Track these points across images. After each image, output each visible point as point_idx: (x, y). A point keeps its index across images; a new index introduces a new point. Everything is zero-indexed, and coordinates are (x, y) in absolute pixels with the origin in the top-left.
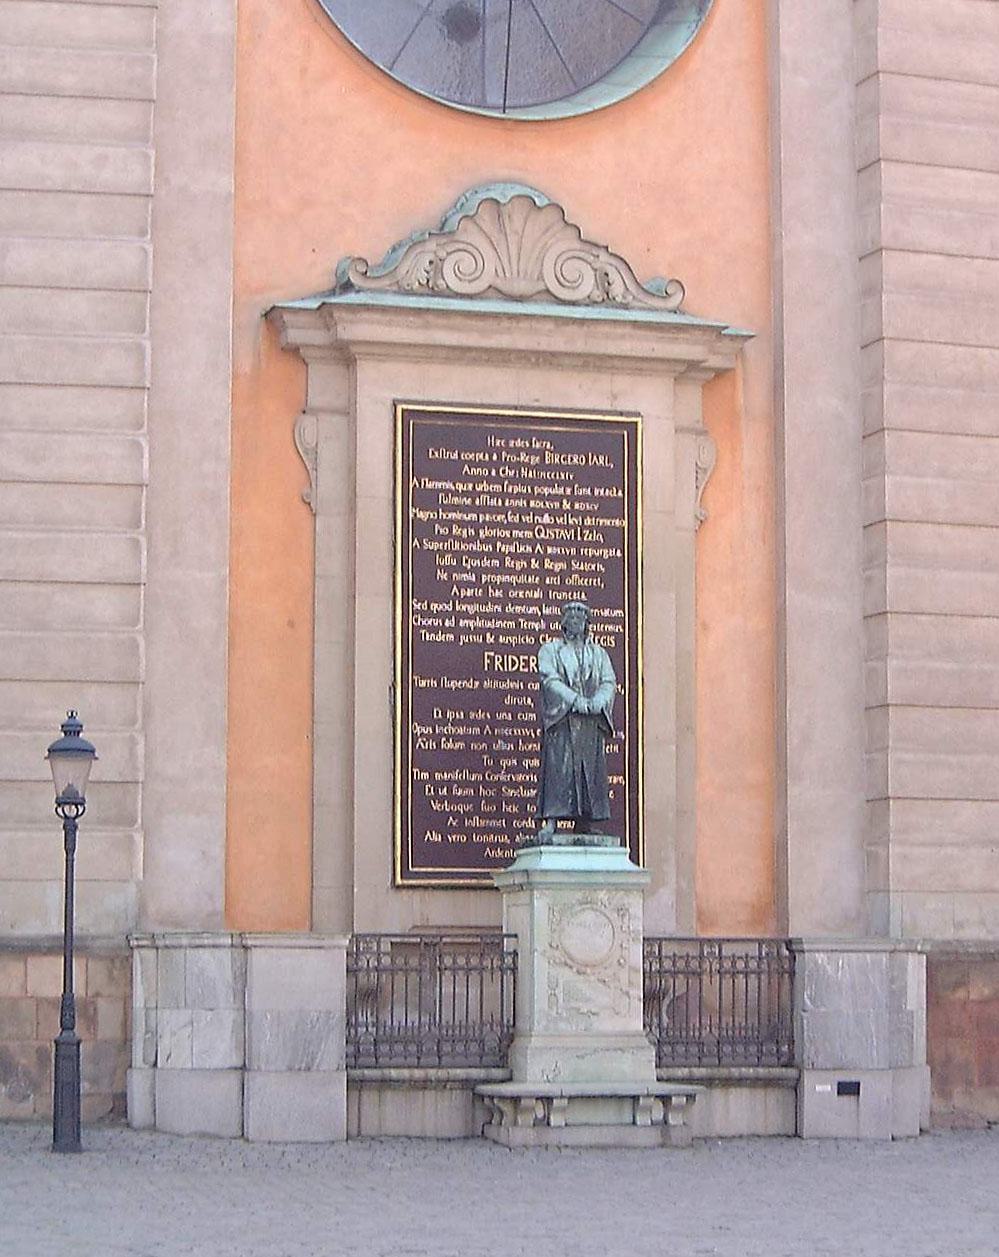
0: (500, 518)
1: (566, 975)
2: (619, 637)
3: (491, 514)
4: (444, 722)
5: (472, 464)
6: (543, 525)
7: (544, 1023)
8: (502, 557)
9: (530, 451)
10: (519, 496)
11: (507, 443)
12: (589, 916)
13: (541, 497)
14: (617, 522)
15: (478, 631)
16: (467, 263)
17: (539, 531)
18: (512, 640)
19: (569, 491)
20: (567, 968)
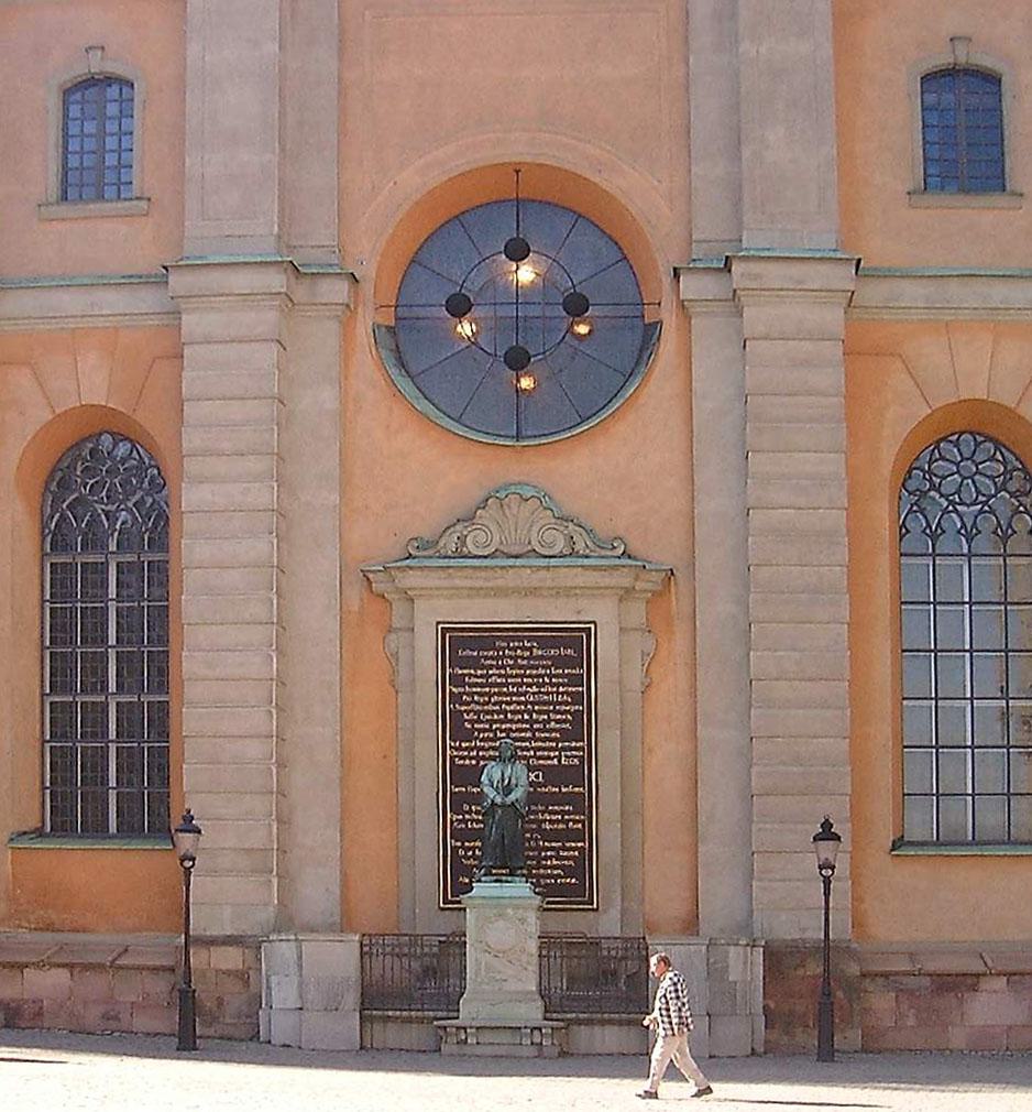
0: (505, 689)
5: (486, 658)
8: (506, 712)
9: (523, 648)
10: (517, 676)
12: (501, 923)
13: (530, 676)
14: (580, 689)
16: (482, 538)
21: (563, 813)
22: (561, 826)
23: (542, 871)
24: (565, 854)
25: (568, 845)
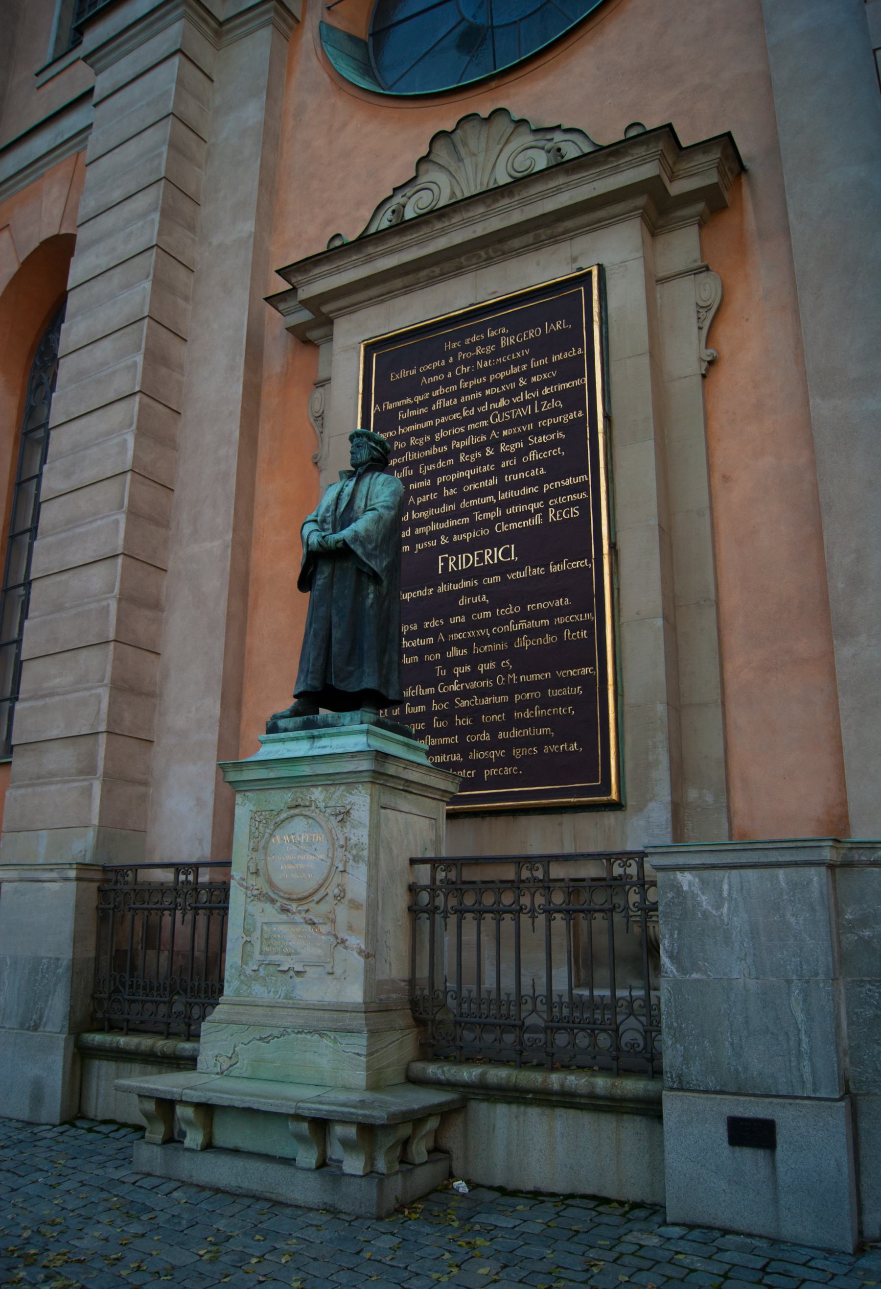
0: (456, 416)
2: (582, 504)
3: (445, 415)
6: (496, 410)
7: (236, 983)
9: (483, 343)
11: (463, 344)
12: (299, 824)
13: (498, 383)
15: (435, 535)
17: (495, 417)
18: (467, 536)
19: (524, 367)
21: (552, 613)
22: (549, 639)
23: (516, 733)
24: (557, 693)
25: (561, 674)
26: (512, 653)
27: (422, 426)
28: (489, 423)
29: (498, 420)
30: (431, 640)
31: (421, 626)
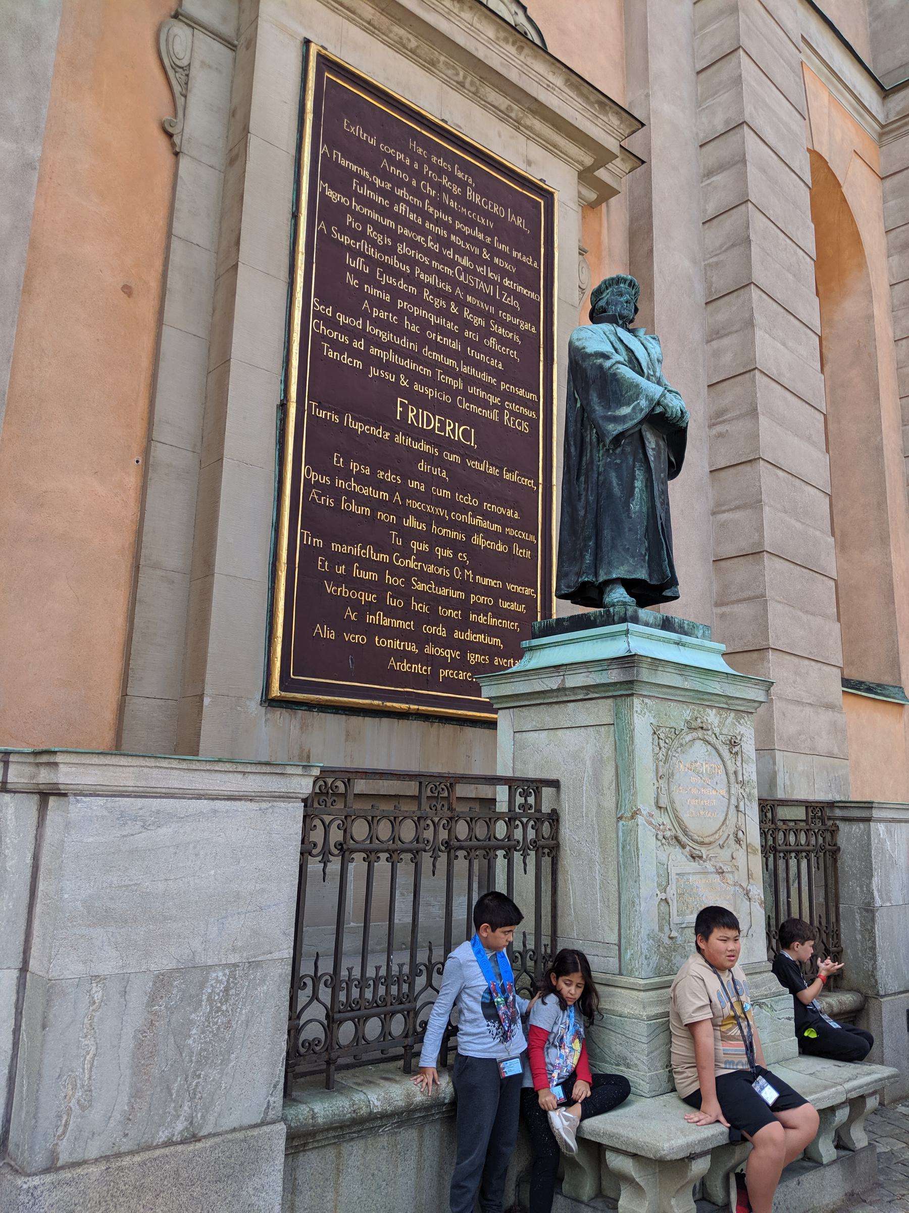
1: (678, 859)
4: (347, 475)
5: (392, 160)
8: (420, 285)
9: (453, 178)
10: (438, 222)
15: (389, 366)
18: (430, 393)
20: (678, 849)
21: (504, 521)
22: (501, 548)
24: (506, 605)
26: (467, 547)
27: (381, 219)
28: (454, 274)
29: (462, 278)
30: (385, 495)
31: (374, 473)
